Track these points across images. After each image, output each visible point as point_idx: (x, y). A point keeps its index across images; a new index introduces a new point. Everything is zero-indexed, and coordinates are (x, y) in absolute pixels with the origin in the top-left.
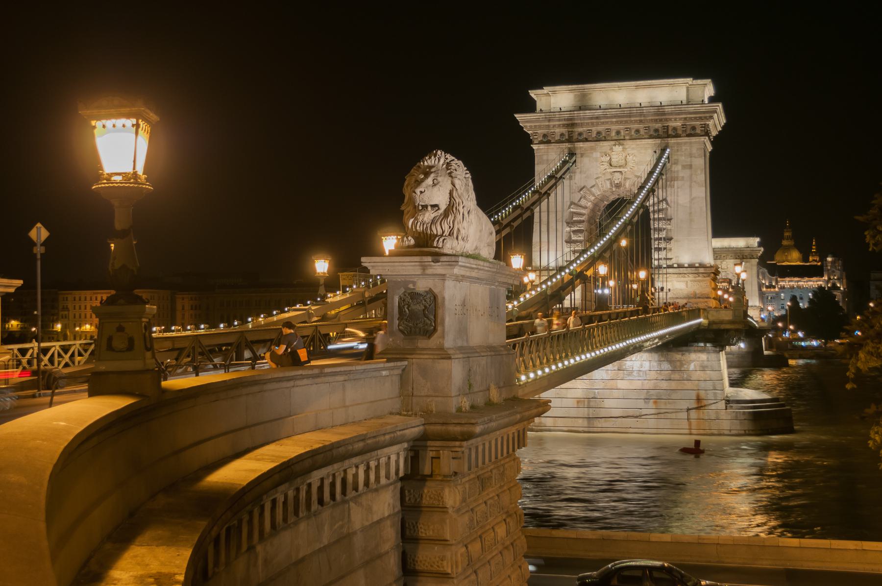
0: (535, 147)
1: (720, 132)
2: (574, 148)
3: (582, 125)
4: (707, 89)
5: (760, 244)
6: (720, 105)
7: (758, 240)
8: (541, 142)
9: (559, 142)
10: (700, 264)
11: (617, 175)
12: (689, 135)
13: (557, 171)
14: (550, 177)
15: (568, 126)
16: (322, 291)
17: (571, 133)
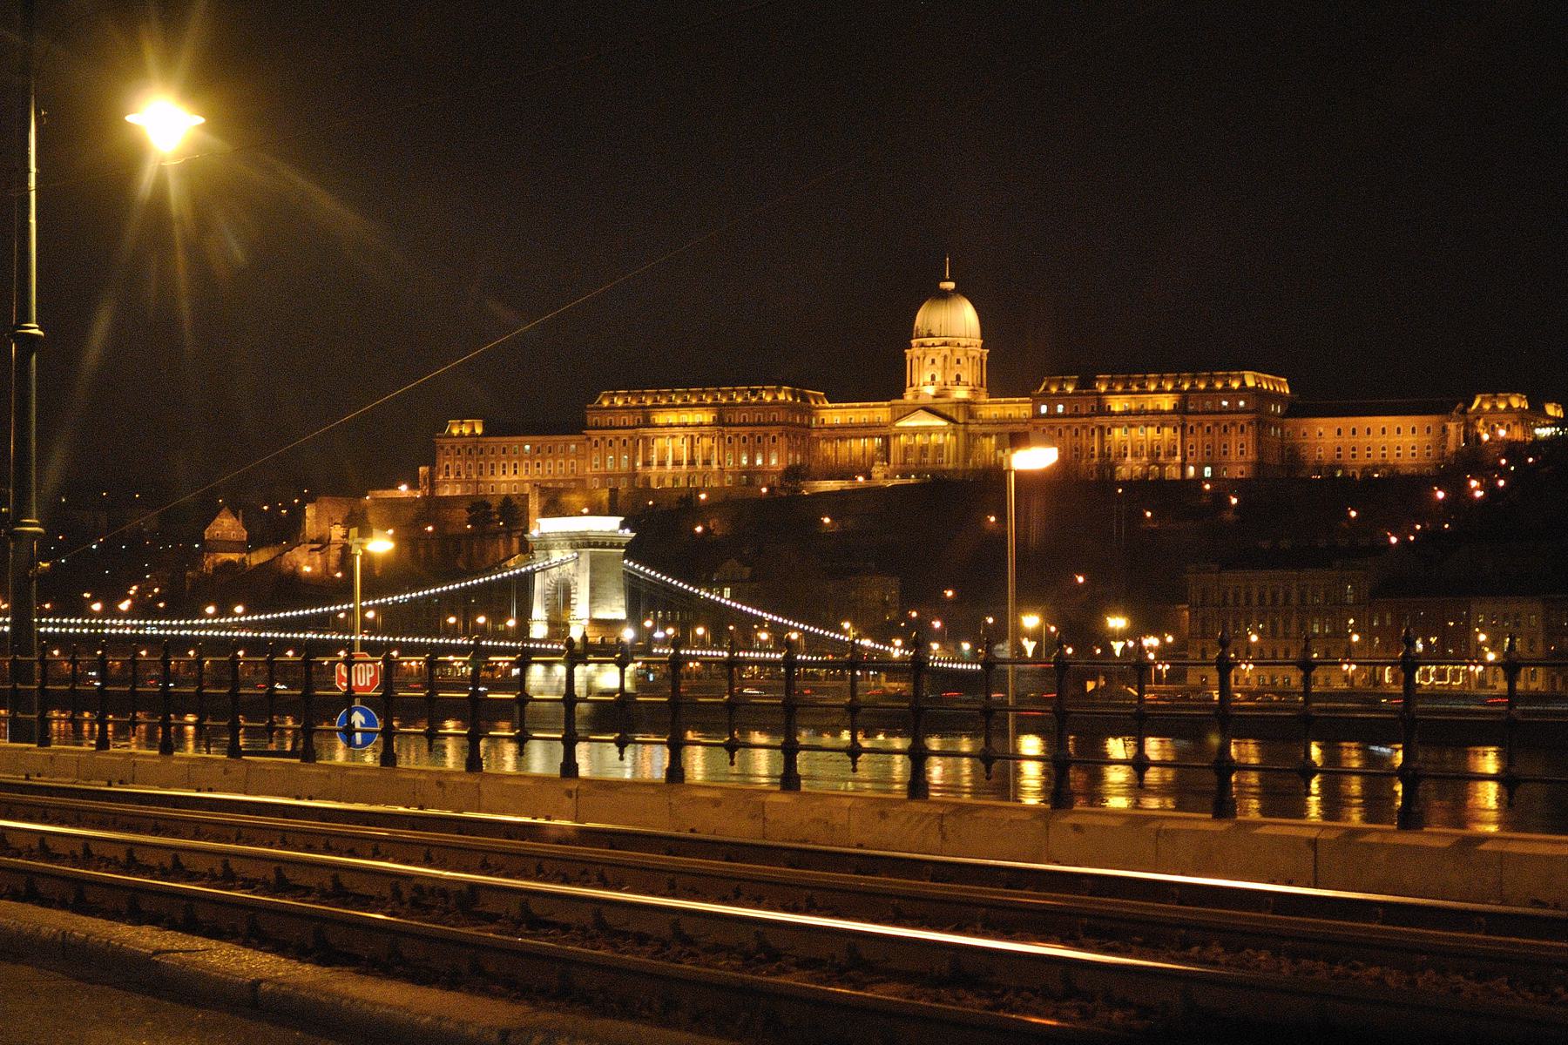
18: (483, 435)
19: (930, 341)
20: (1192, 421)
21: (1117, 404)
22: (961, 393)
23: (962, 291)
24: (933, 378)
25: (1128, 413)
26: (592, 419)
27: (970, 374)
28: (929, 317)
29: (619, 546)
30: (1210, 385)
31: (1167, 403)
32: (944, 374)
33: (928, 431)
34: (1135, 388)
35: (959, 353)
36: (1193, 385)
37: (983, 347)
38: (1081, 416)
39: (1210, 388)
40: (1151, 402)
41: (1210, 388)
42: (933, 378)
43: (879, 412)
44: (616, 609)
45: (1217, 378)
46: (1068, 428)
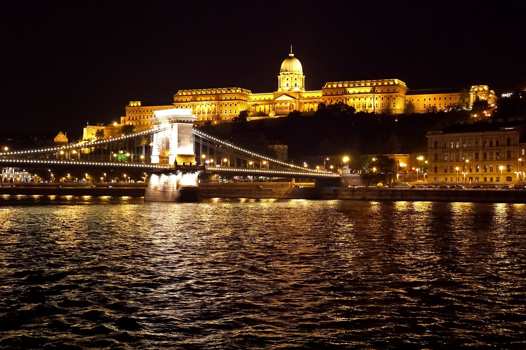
18: (142, 105)
19: (286, 73)
20: (376, 95)
21: (351, 90)
22: (297, 89)
24: (288, 85)
26: (176, 99)
27: (300, 83)
28: (285, 65)
29: (191, 122)
33: (286, 102)
35: (296, 76)
37: (303, 75)
38: (339, 95)
39: (383, 85)
40: (362, 90)
41: (383, 85)
42: (288, 85)
43: (270, 96)
44: (189, 149)
45: (385, 81)
46: (334, 99)
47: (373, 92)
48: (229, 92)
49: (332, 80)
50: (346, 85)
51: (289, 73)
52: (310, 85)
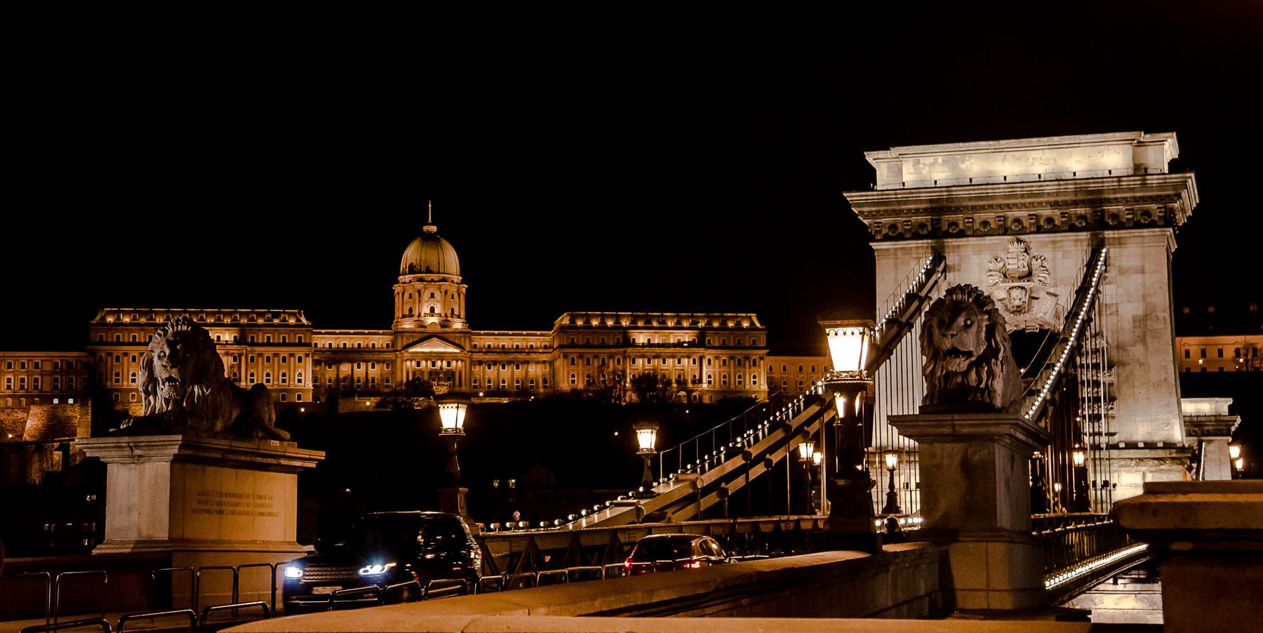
0: (874, 245)
1: (1189, 218)
2: (943, 247)
3: (957, 210)
4: (1167, 148)
5: (1232, 410)
6: (1193, 175)
7: (1230, 401)
8: (886, 238)
9: (916, 236)
10: (1165, 443)
11: (1015, 293)
12: (1138, 225)
13: (921, 286)
14: (910, 297)
15: (932, 209)
16: (647, 475)
17: (936, 223)
20: (709, 354)
21: (641, 338)
23: (448, 232)
24: (432, 310)
25: (650, 345)
27: (459, 307)
28: (411, 254)
30: (724, 323)
31: (687, 336)
32: (444, 307)
33: (441, 356)
34: (655, 324)
36: (709, 323)
39: (724, 327)
41: (724, 327)
42: (432, 310)
47: (700, 342)
48: (276, 321)
49: (572, 306)
50: (625, 323)
51: (435, 277)
52: (479, 317)
